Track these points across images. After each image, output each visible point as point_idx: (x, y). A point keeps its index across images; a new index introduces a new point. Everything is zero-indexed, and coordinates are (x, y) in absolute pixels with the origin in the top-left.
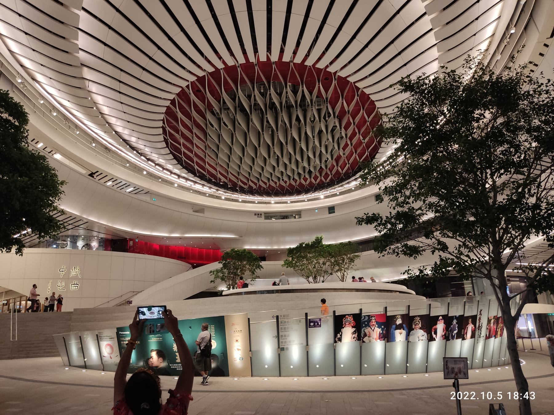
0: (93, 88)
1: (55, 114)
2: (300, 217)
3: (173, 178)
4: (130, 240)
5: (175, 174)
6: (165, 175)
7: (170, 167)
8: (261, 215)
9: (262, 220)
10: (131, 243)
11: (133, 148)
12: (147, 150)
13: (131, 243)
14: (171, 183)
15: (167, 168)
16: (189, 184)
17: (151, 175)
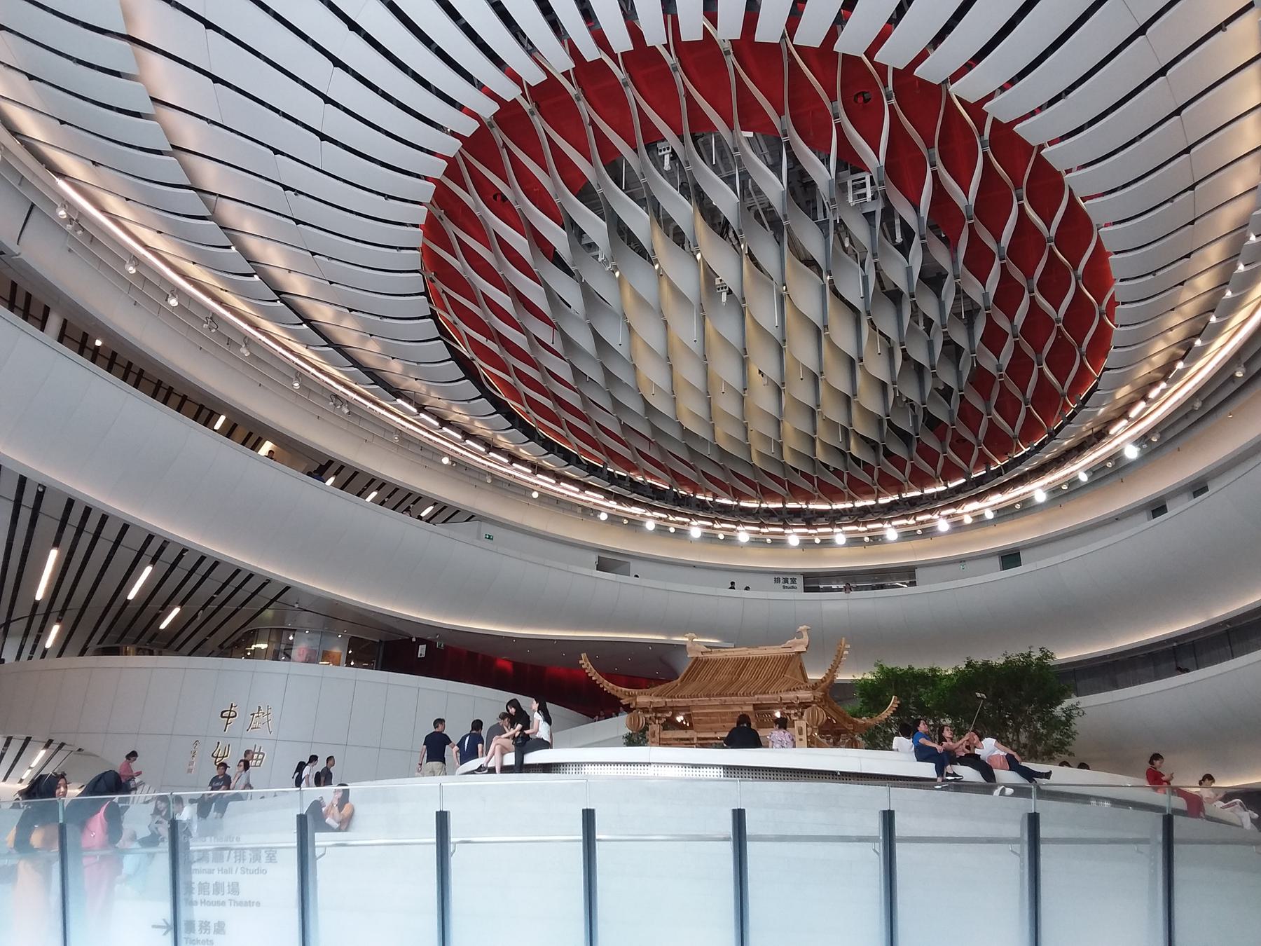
0: (246, 221)
1: (173, 302)
2: (913, 584)
3: (520, 473)
4: (421, 641)
5: (524, 462)
6: (496, 464)
7: (479, 428)
8: (794, 581)
9: (800, 595)
10: (422, 650)
11: (397, 393)
12: (434, 400)
13: (422, 650)
14: (518, 491)
15: (478, 432)
16: (569, 491)
17: (459, 466)
